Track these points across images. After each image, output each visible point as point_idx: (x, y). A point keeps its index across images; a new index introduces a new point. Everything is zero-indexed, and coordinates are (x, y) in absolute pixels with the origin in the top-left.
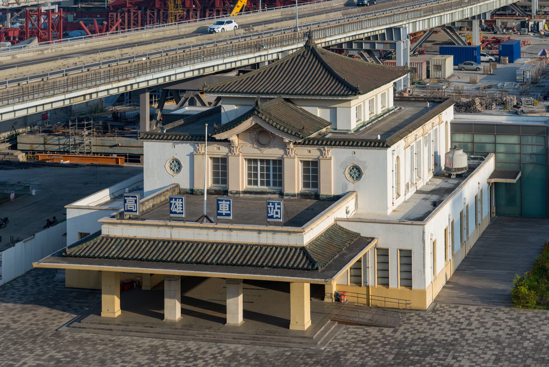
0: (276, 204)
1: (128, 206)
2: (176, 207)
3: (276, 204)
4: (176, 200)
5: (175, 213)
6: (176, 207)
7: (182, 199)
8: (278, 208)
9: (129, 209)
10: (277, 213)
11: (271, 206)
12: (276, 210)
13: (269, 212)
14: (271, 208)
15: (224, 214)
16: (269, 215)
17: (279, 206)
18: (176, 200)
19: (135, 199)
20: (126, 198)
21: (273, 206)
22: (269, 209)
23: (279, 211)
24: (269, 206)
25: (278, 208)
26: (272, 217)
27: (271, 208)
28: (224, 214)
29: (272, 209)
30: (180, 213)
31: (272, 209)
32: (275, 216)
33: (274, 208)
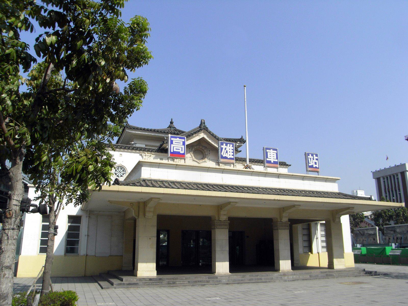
0: (314, 155)
1: (175, 148)
2: (227, 152)
3: (314, 155)
4: (226, 145)
5: (226, 158)
6: (227, 152)
7: (233, 144)
8: (317, 159)
9: (175, 150)
10: (316, 163)
11: (310, 156)
12: (315, 161)
13: (310, 162)
14: (310, 159)
15: (272, 162)
16: (310, 165)
17: (317, 158)
18: (226, 145)
19: (183, 140)
20: (172, 139)
21: (312, 157)
22: (309, 159)
23: (317, 161)
24: (309, 157)
25: (317, 159)
26: (312, 167)
27: (310, 159)
28: (272, 162)
29: (312, 159)
30: (230, 159)
31: (312, 159)
32: (314, 166)
33: (313, 159)
